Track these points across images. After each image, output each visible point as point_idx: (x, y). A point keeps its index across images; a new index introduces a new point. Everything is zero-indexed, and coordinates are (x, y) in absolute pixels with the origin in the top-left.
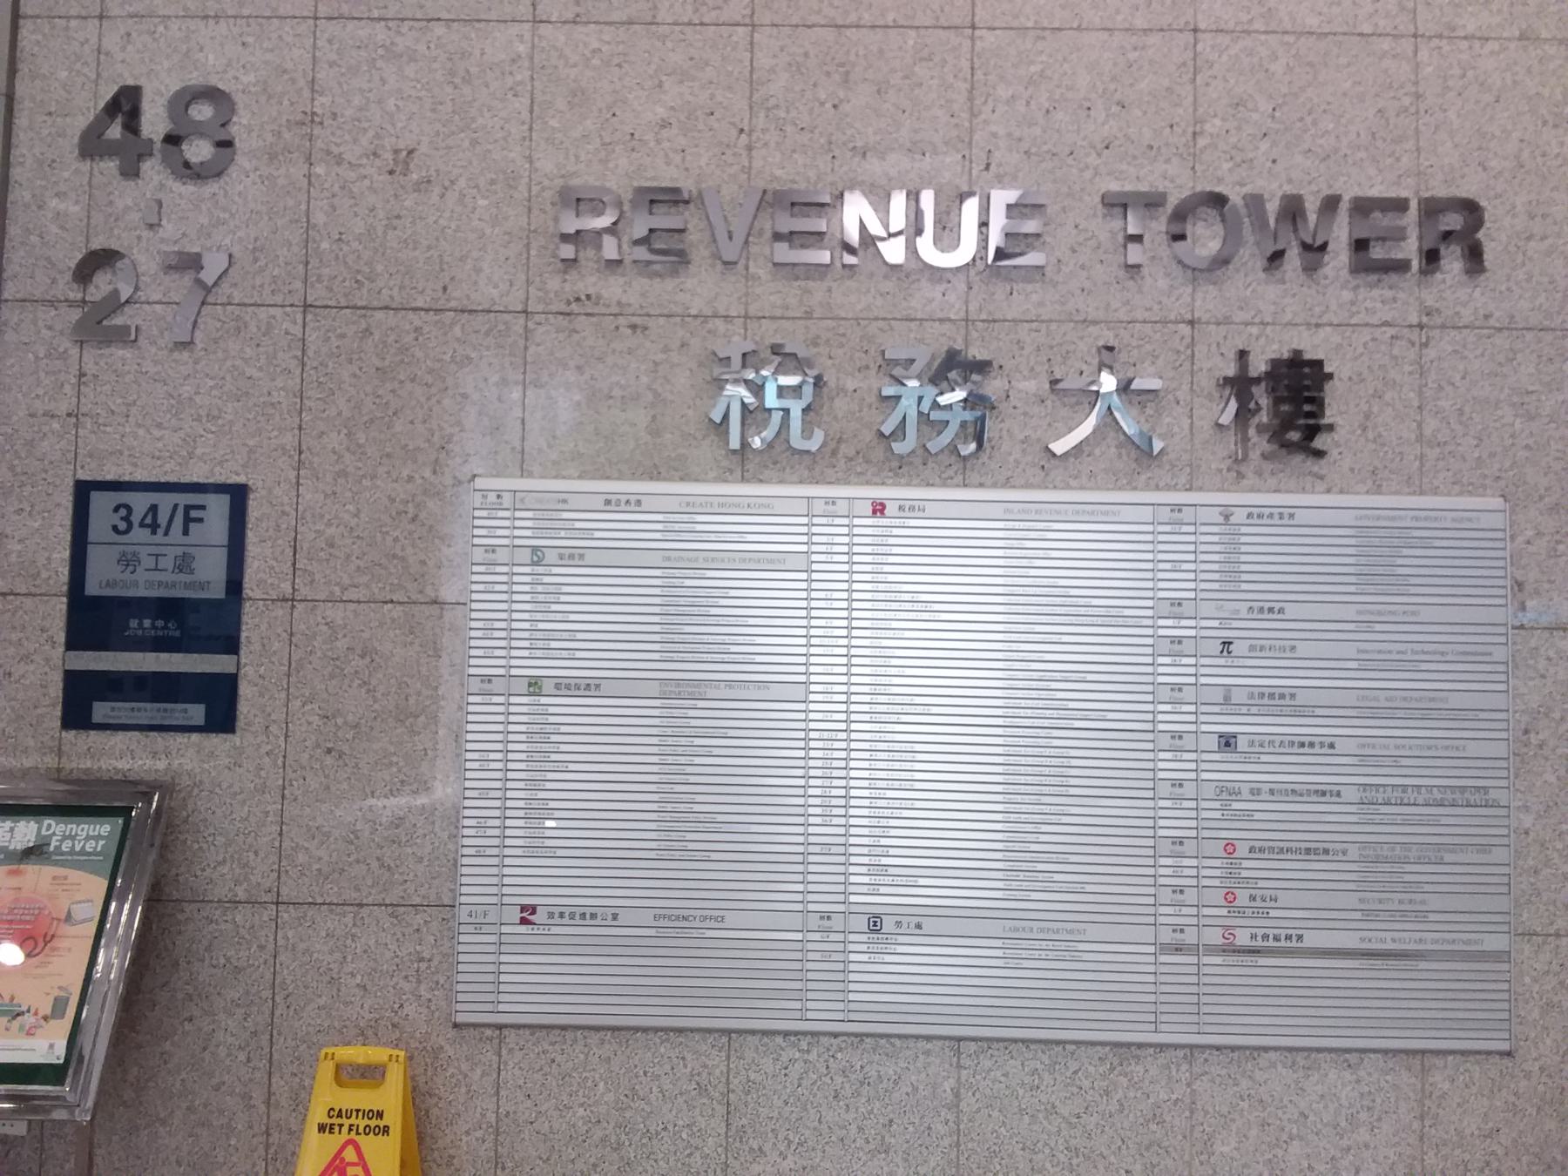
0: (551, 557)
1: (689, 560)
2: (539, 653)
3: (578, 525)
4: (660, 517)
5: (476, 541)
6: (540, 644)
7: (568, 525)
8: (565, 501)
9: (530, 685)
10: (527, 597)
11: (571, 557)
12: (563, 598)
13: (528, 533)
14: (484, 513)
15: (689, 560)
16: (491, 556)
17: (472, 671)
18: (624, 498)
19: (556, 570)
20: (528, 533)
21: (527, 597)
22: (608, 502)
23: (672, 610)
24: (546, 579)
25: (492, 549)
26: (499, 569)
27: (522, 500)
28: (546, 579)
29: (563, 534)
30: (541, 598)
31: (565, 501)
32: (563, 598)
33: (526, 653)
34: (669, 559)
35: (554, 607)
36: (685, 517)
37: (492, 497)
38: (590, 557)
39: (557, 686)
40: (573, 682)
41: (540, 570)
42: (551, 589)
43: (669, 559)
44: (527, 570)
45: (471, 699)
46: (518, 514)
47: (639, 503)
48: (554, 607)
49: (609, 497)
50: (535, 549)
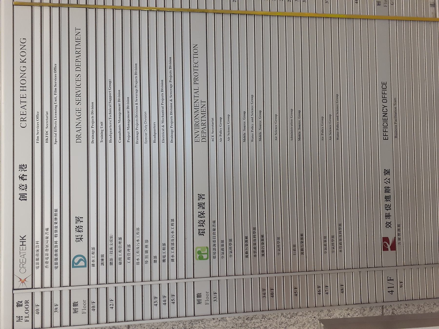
0: (80, 249)
1: (79, 117)
2: (172, 253)
3: (47, 225)
4: (37, 147)
5: (66, 322)
6: (164, 253)
7: (47, 234)
8: (23, 239)
9: (201, 258)
10: (120, 268)
11: (79, 229)
12: (120, 234)
13: (56, 273)
14: (38, 318)
15: (79, 117)
16: (80, 307)
17: (190, 312)
18: (18, 182)
19: (93, 244)
20: (56, 273)
21: (120, 268)
22: (23, 197)
23: (128, 132)
24: (102, 251)
25: (73, 306)
26: (93, 298)
27: (23, 281)
28: (102, 251)
29: (57, 239)
30: (120, 255)
31: (23, 239)
32: (120, 234)
33: (173, 265)
34: (78, 137)
35: (129, 241)
36: (37, 122)
37: (20, 312)
38: (79, 210)
39: (202, 233)
40: (197, 219)
41: (93, 258)
42: (111, 245)
43: (78, 137)
44: (93, 270)
45: (215, 310)
46: (37, 284)
47: (22, 167)
48: (129, 241)
49: (17, 196)
50: (72, 265)
